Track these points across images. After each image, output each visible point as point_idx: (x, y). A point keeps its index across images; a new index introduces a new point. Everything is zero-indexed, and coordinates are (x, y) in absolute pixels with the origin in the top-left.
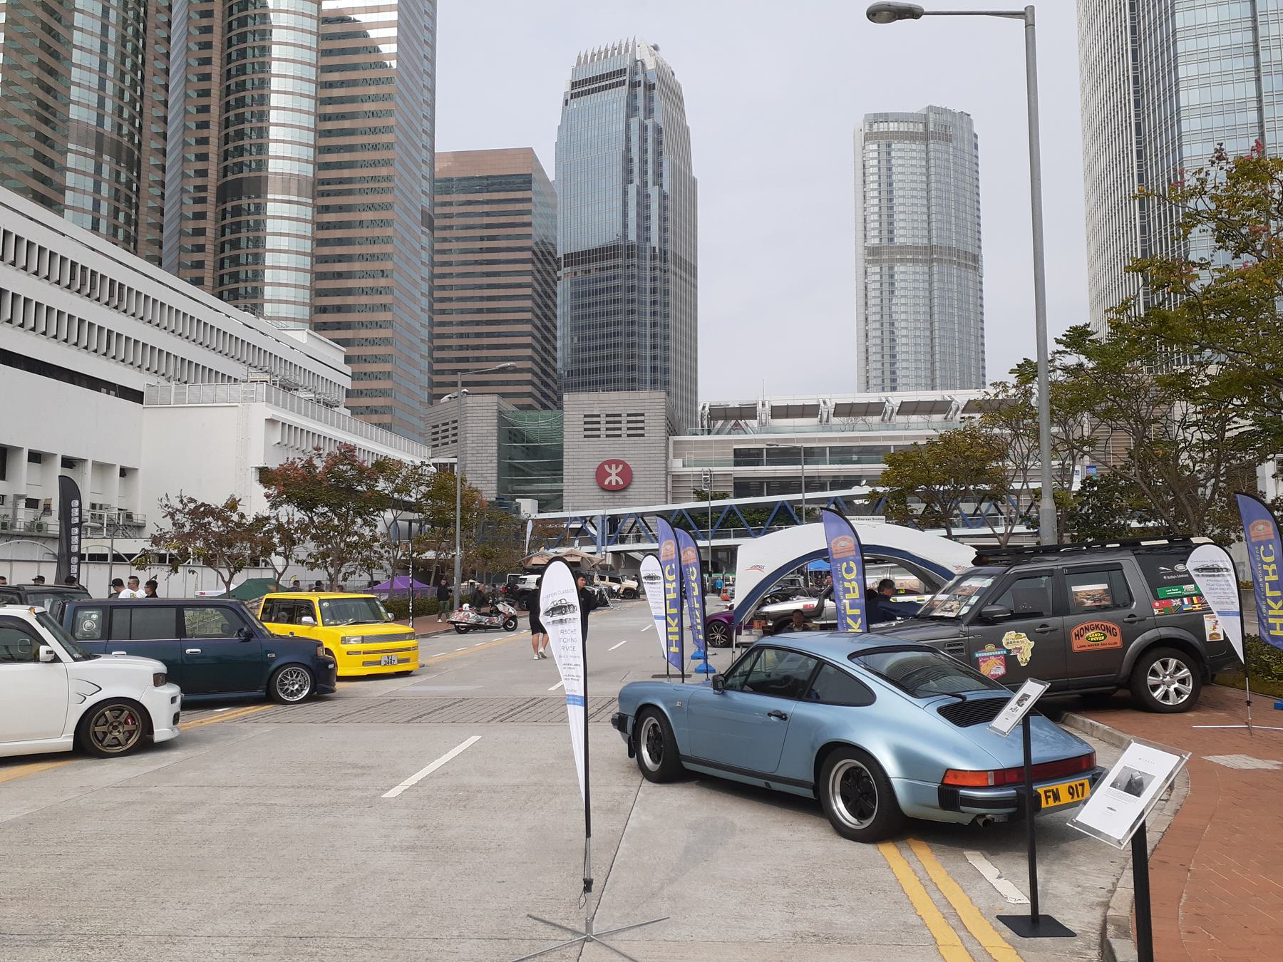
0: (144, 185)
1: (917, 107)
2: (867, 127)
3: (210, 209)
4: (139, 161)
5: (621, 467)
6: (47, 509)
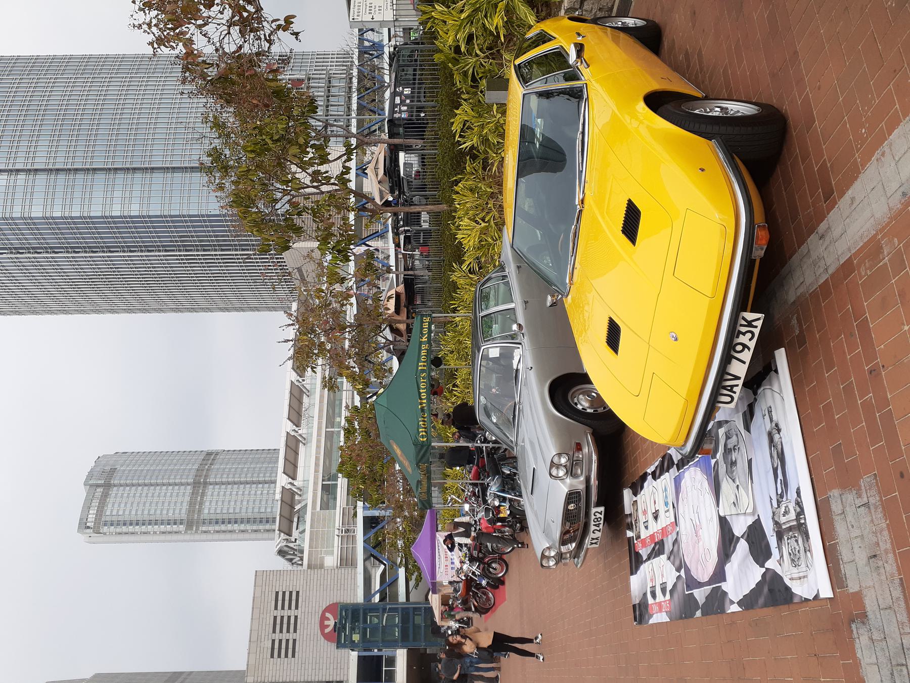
1: (81, 493)
2: (88, 531)
5: (328, 615)
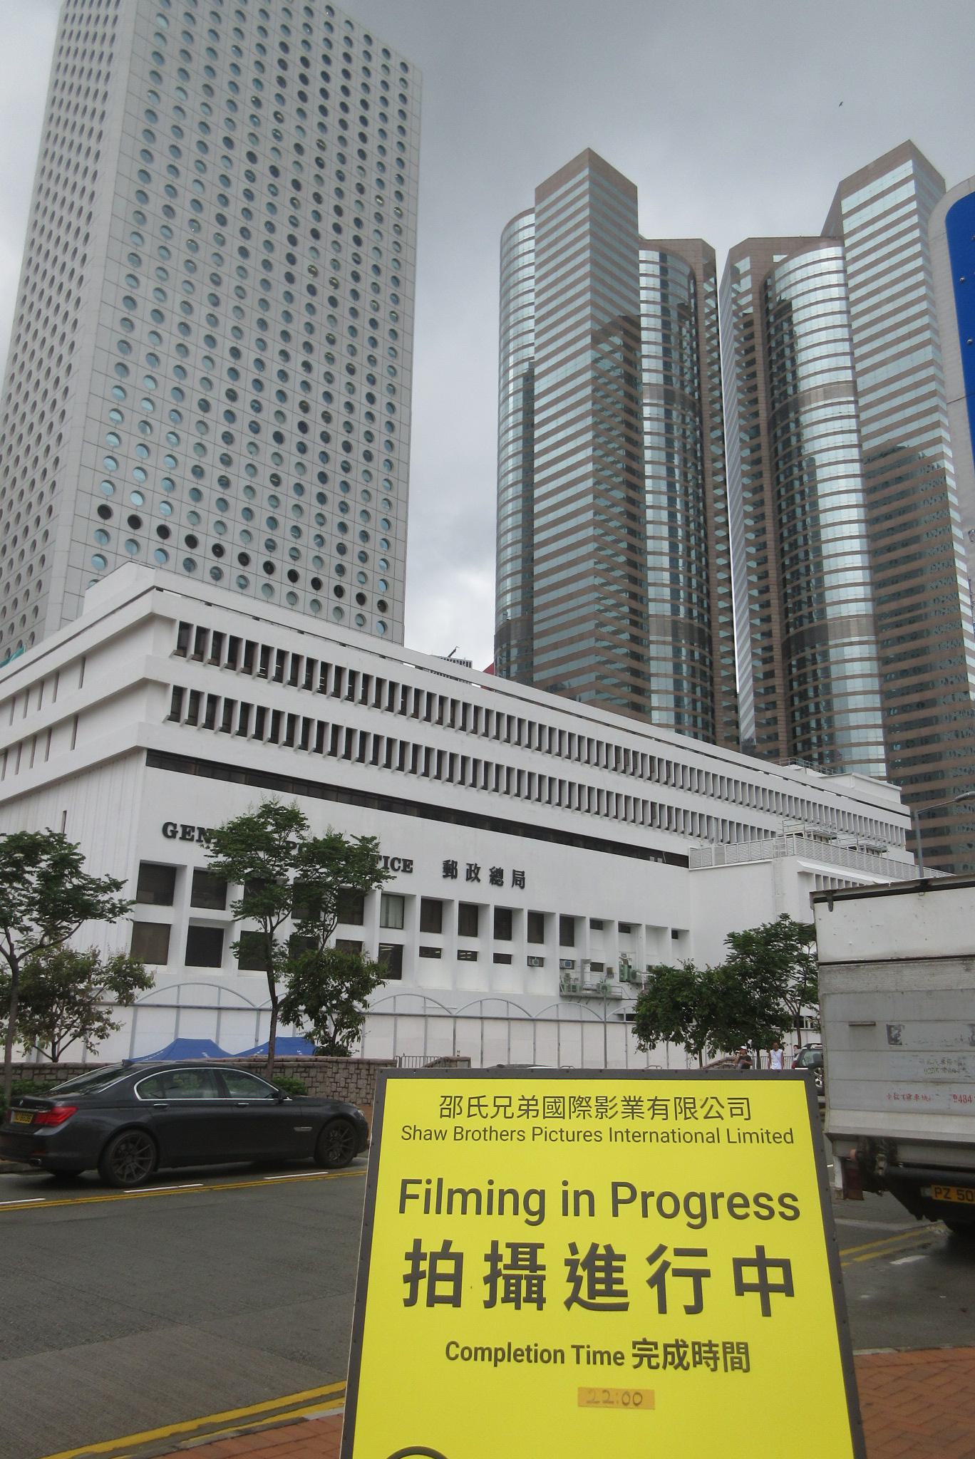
0: (716, 657)
3: (777, 666)
4: (710, 637)
6: (610, 972)
